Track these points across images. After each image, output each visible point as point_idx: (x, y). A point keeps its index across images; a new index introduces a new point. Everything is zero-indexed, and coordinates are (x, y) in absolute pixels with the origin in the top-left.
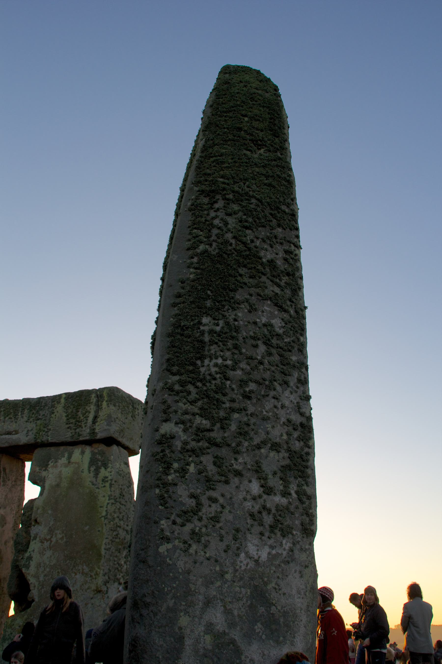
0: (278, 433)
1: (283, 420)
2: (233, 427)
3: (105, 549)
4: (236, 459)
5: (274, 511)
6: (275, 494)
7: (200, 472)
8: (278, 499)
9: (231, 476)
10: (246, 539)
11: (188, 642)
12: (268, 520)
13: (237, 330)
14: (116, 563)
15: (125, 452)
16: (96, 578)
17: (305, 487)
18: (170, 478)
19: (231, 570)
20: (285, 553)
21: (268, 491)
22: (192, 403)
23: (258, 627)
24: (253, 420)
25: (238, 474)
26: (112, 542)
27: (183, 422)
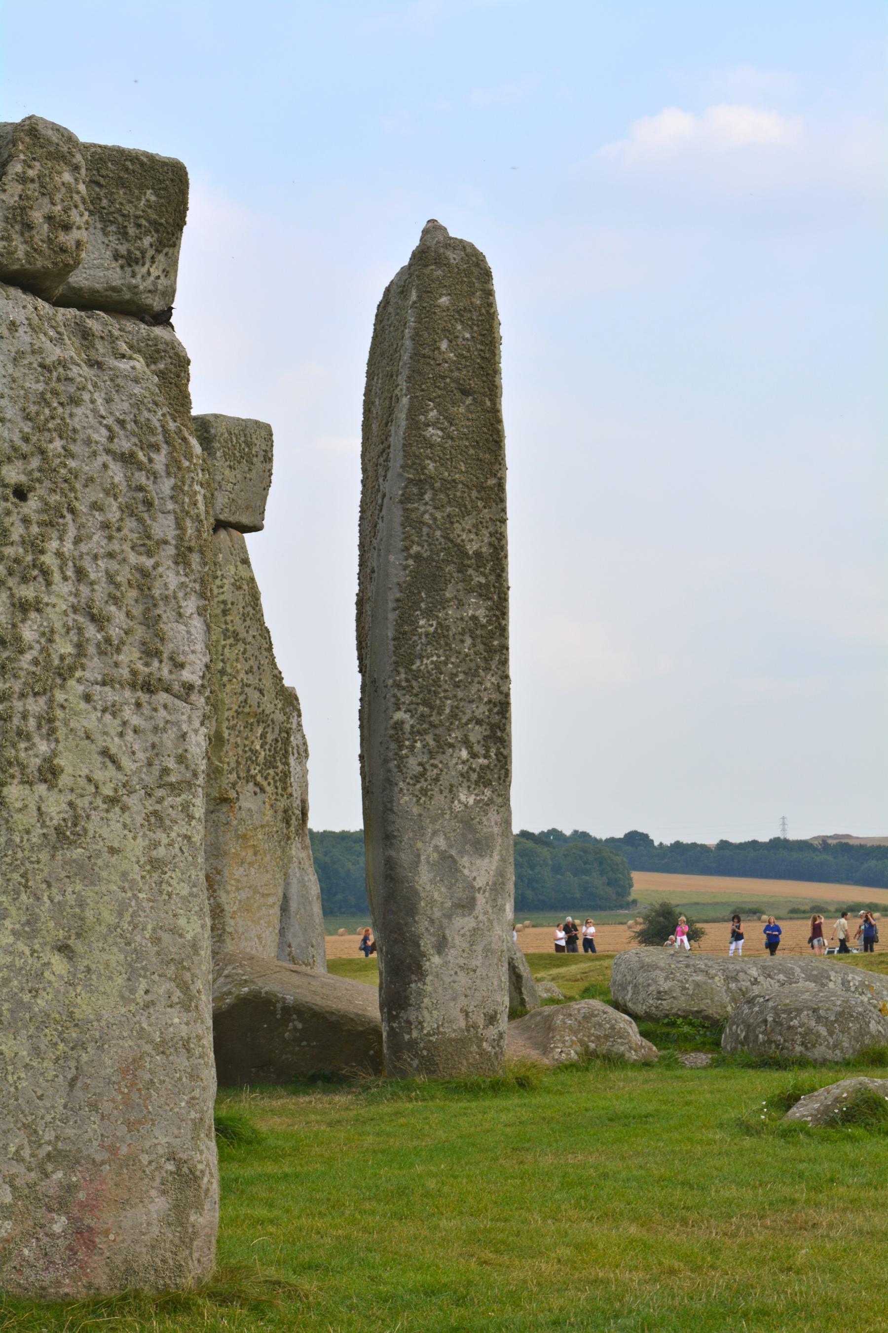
0: (481, 711)
1: (486, 700)
2: (447, 711)
3: (228, 728)
4: (450, 735)
5: (478, 770)
6: (479, 758)
7: (424, 747)
8: (481, 761)
9: (446, 747)
10: (458, 791)
11: (423, 858)
12: (474, 776)
13: (448, 628)
14: (247, 749)
15: (235, 533)
16: (216, 779)
17: (502, 750)
18: (404, 752)
19: (448, 812)
20: (486, 799)
21: (474, 755)
22: (416, 695)
23: (468, 847)
24: (462, 704)
25: (451, 746)
26: (238, 714)
27: (410, 711)
